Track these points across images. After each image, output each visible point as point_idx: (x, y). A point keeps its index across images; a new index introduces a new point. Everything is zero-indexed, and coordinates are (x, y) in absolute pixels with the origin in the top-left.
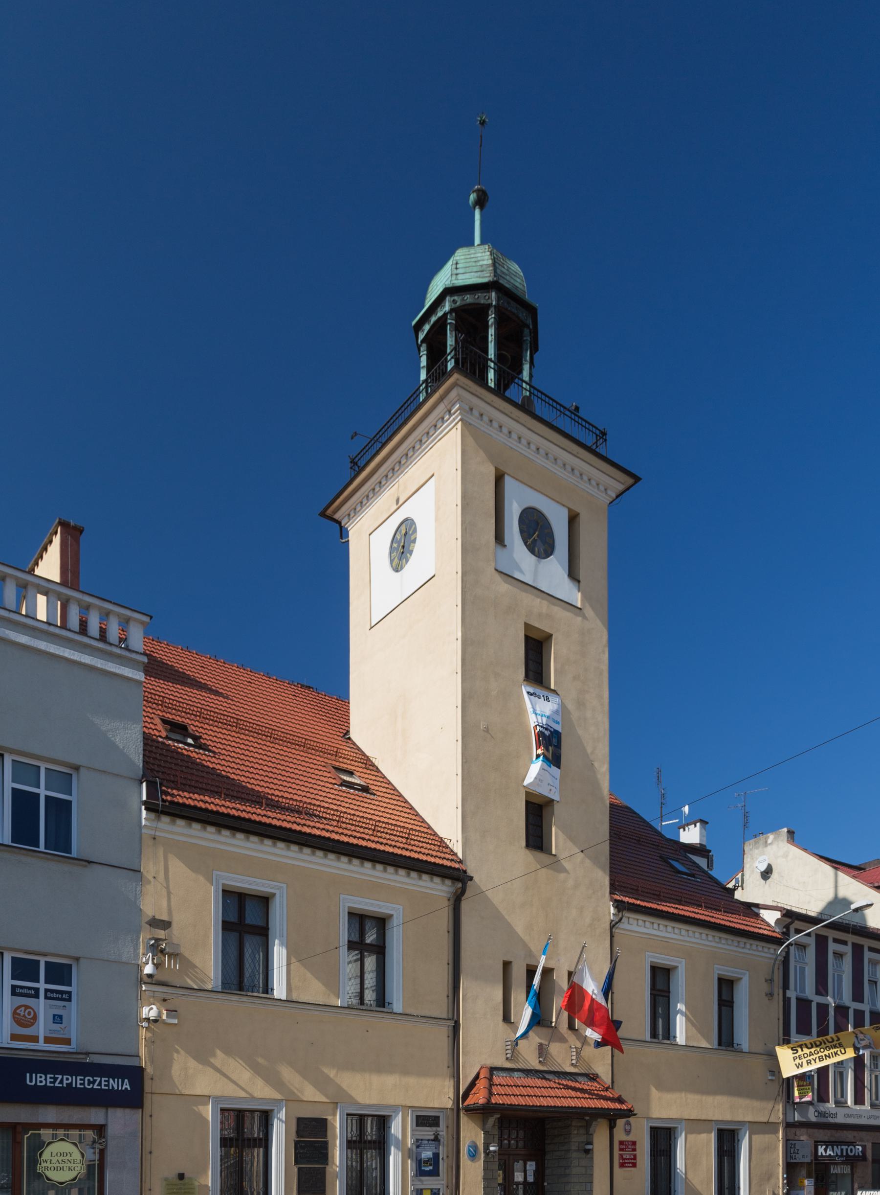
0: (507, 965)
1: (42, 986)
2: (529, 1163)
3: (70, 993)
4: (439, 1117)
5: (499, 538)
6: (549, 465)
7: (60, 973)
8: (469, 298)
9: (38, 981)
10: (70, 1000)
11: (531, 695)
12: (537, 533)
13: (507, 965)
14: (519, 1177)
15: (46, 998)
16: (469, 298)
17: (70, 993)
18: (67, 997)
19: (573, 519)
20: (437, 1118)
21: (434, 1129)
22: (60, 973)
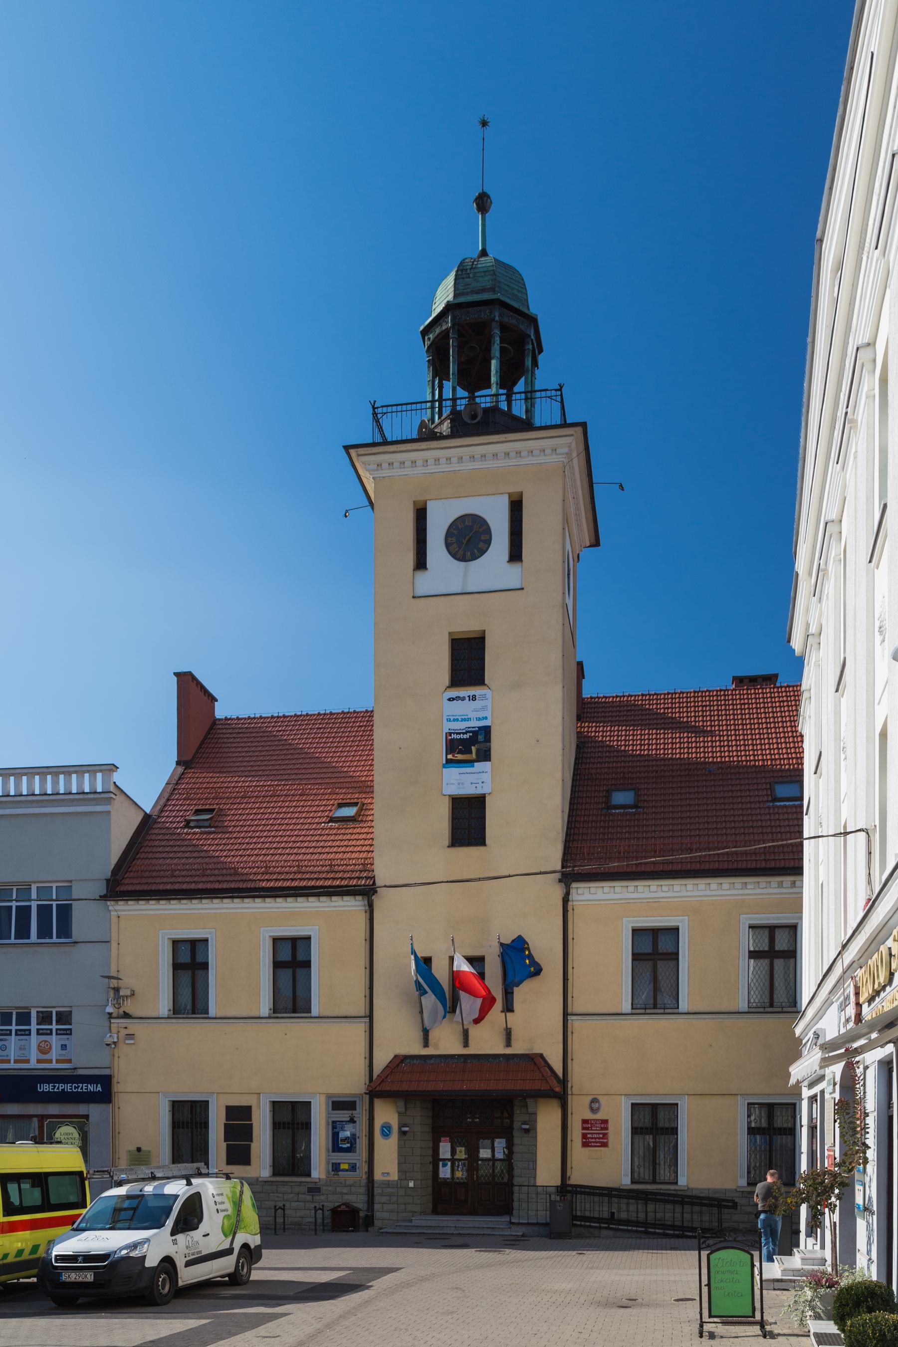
1: (54, 1027)
2: (497, 1141)
3: (70, 1029)
4: (355, 1102)
6: (477, 465)
7: (64, 1018)
9: (51, 1024)
10: (30, 1034)
11: (454, 699)
14: (485, 1153)
15: (57, 1034)
17: (30, 1030)
18: (69, 1032)
19: (516, 507)
21: (350, 1112)
22: (64, 1018)
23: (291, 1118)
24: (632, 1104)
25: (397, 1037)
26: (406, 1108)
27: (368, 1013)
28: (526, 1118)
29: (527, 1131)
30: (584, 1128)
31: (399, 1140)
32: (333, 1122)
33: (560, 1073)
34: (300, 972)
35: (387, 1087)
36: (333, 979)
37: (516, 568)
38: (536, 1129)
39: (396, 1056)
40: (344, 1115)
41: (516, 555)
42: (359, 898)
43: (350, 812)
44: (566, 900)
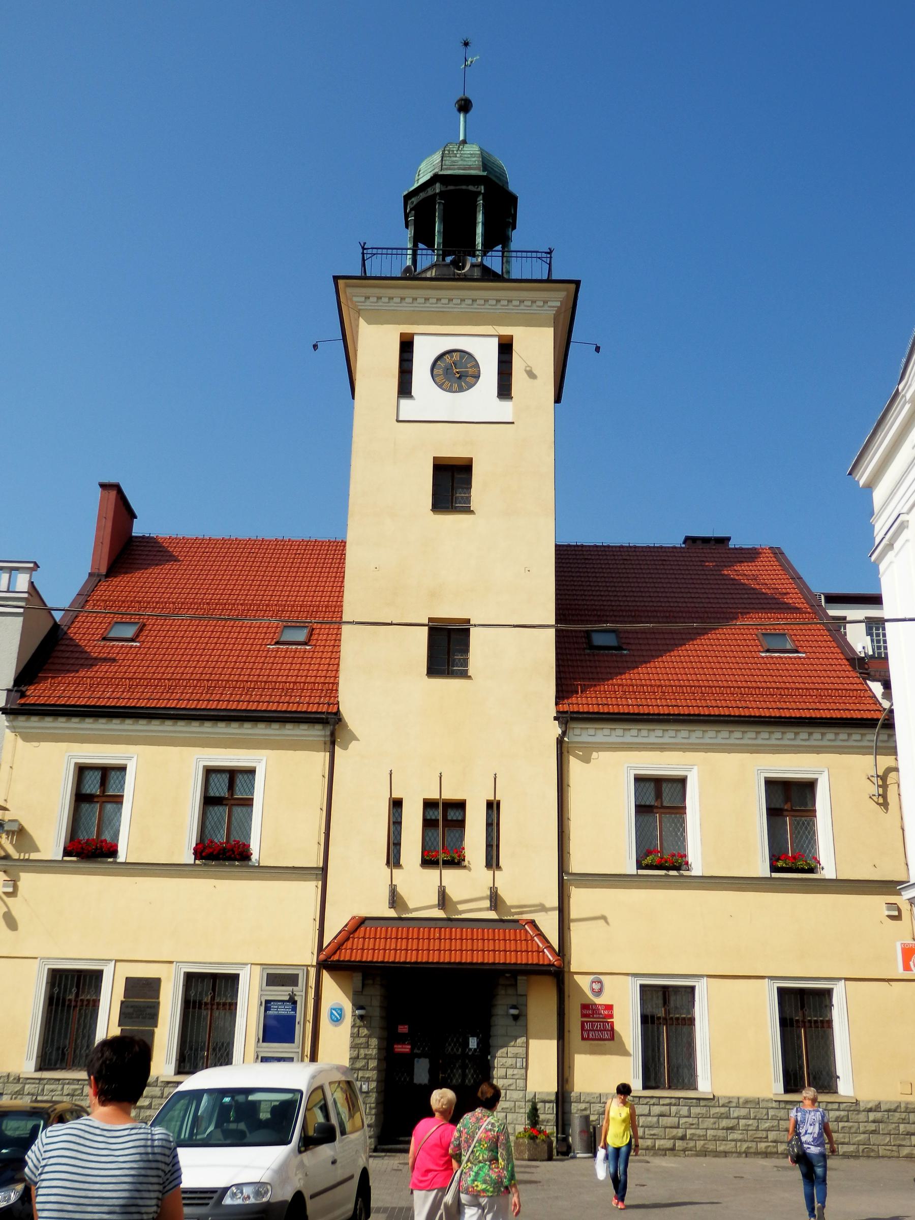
0: (397, 804)
5: (405, 389)
8: (422, 195)
12: (455, 371)
13: (397, 804)
16: (422, 195)
20: (296, 976)
21: (290, 988)
23: (209, 995)
24: (642, 986)
25: (361, 891)
26: (364, 985)
27: (321, 865)
28: (513, 1001)
29: (516, 1018)
30: (583, 1016)
31: (353, 1026)
32: (267, 1002)
33: (555, 944)
34: (238, 811)
35: (345, 955)
36: (277, 823)
37: (507, 405)
38: (526, 1016)
39: (353, 918)
40: (281, 993)
41: (505, 390)
42: (319, 726)
43: (302, 635)
44: (560, 742)
